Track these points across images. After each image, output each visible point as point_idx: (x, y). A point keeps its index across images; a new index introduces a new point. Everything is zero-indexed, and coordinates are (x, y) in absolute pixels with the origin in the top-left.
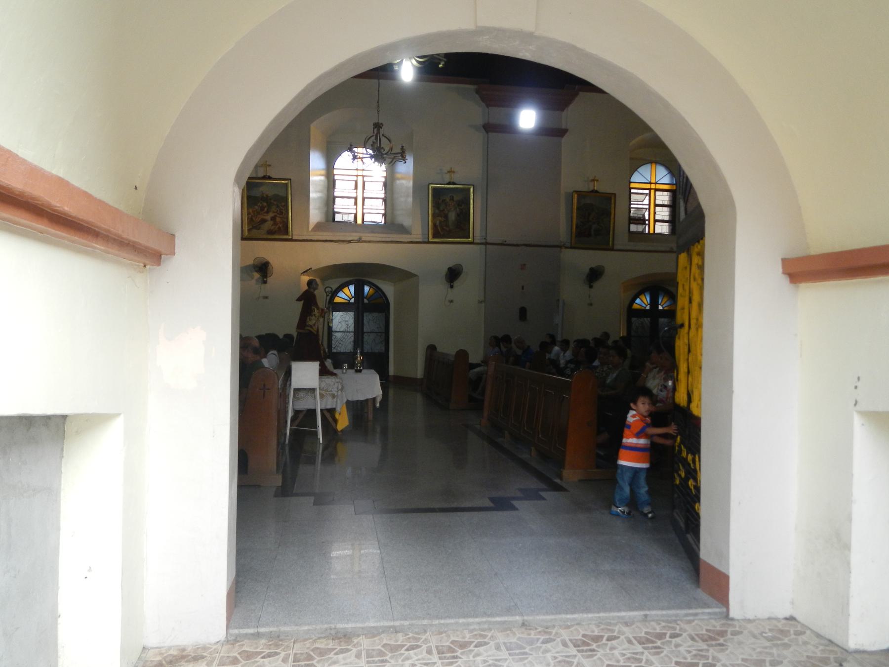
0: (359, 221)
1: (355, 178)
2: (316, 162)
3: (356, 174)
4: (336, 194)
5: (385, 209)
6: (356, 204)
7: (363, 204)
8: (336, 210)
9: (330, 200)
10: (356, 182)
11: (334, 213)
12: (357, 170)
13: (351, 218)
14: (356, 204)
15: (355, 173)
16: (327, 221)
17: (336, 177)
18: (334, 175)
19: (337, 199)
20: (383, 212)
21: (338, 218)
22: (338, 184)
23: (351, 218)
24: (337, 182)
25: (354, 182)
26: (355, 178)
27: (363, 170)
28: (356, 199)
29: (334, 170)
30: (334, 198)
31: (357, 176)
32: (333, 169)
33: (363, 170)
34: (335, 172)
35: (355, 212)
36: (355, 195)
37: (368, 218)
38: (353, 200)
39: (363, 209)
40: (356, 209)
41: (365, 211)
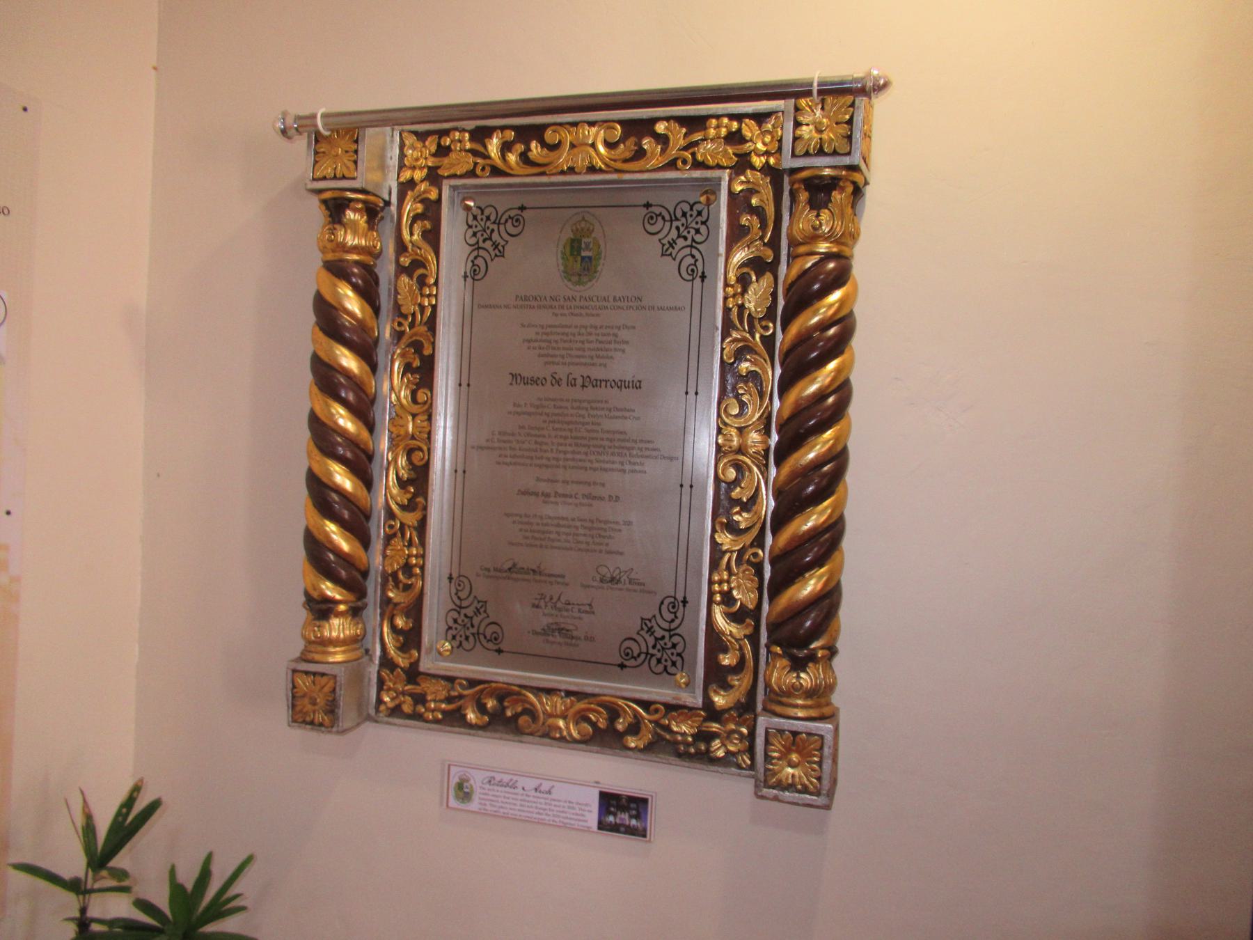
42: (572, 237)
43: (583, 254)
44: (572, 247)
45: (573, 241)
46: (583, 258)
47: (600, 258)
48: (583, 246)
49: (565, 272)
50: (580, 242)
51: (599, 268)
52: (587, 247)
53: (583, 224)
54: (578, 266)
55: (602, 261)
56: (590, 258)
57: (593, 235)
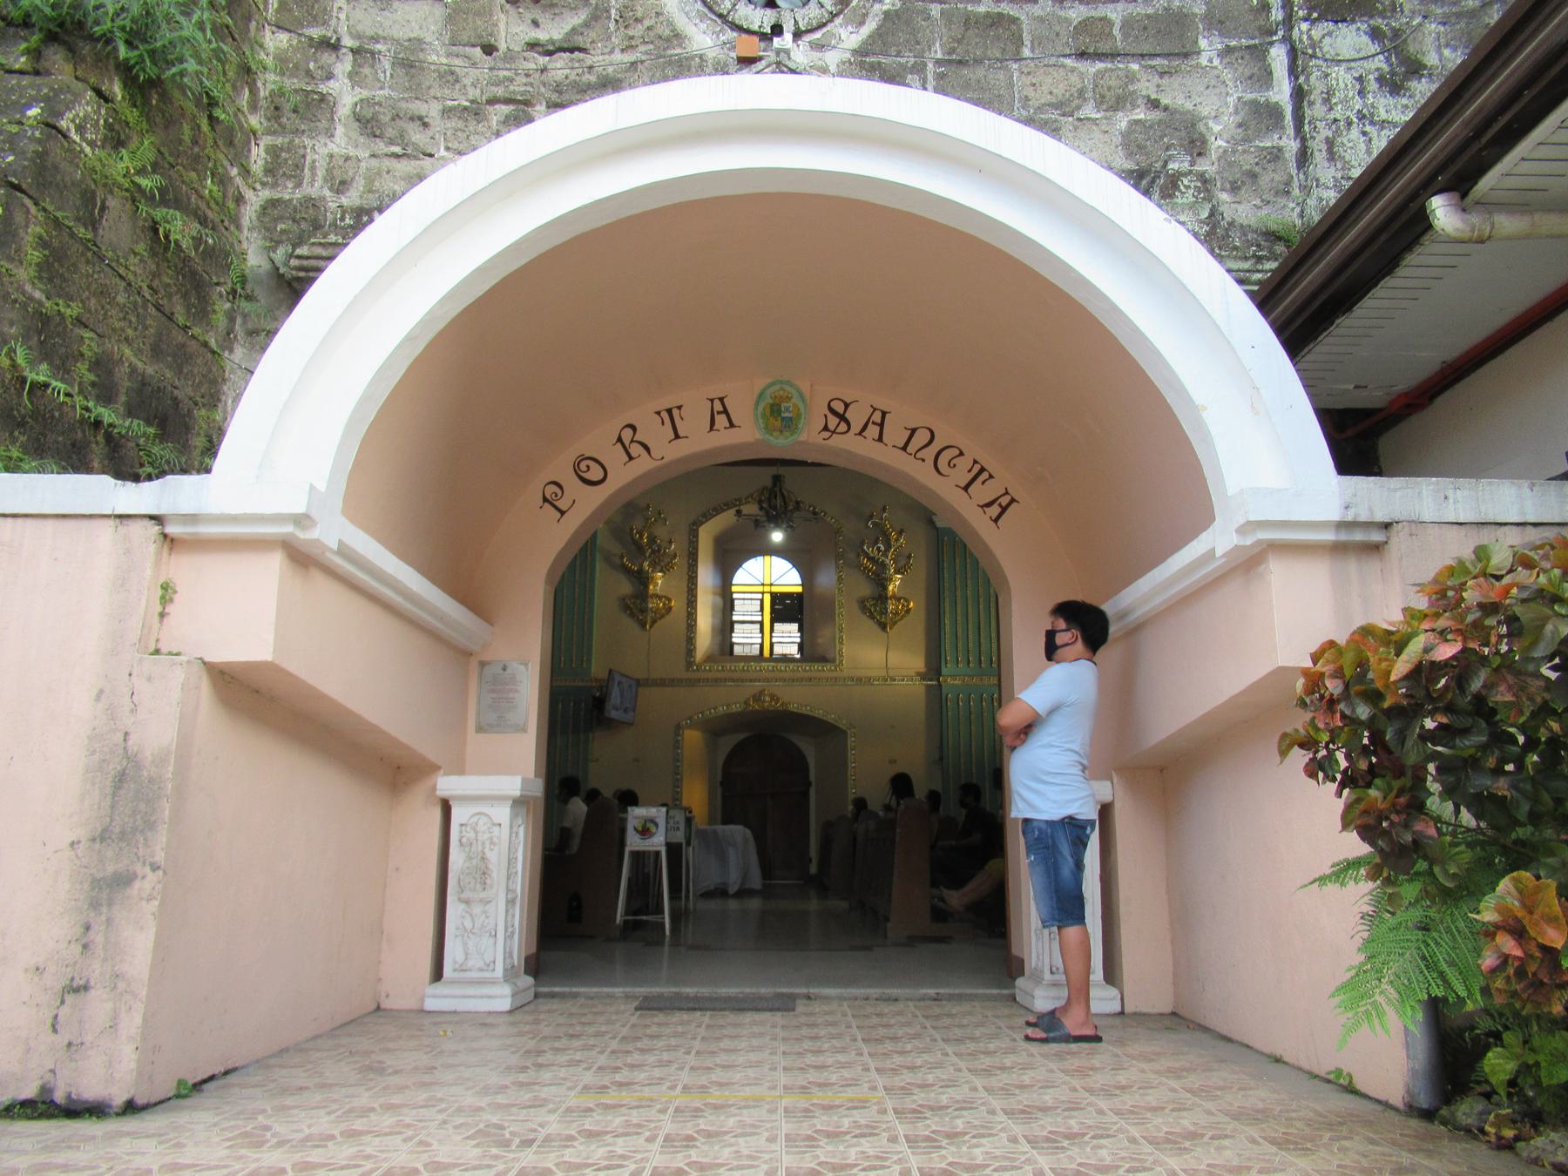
0: (766, 653)
1: (760, 596)
2: (706, 577)
4: (735, 618)
5: (801, 637)
6: (762, 631)
7: (772, 630)
9: (726, 626)
10: (762, 601)
11: (732, 645)
12: (763, 585)
13: (756, 652)
14: (762, 631)
15: (760, 589)
16: (722, 653)
17: (735, 596)
18: (732, 593)
19: (736, 626)
20: (798, 640)
21: (737, 650)
24: (736, 602)
25: (759, 602)
26: (760, 596)
27: (771, 585)
28: (761, 623)
30: (732, 623)
31: (763, 593)
32: (731, 585)
33: (771, 585)
34: (734, 589)
36: (759, 618)
37: (778, 650)
38: (758, 626)
39: (771, 637)
40: (762, 638)
41: (774, 640)
42: (771, 401)
43: (783, 415)
44: (772, 411)
45: (772, 405)
46: (783, 419)
47: (800, 418)
48: (783, 409)
49: (766, 428)
50: (779, 406)
51: (800, 426)
52: (787, 410)
53: (781, 393)
54: (778, 423)
55: (802, 420)
56: (791, 419)
57: (793, 401)
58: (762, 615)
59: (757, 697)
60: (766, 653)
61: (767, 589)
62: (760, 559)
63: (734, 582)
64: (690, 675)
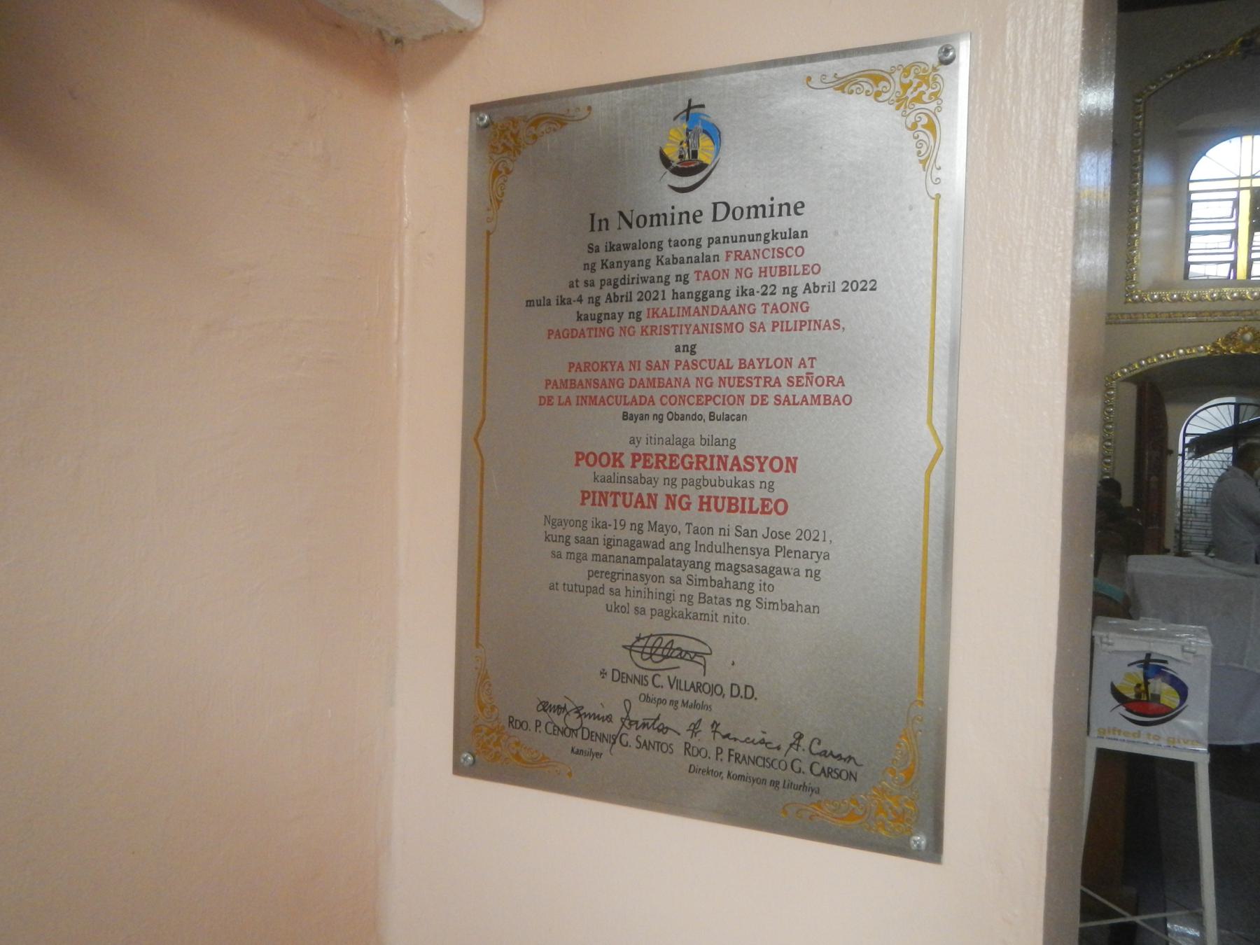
0: (1241, 274)
3: (1237, 186)
8: (1191, 259)
12: (1239, 178)
15: (1235, 184)
19: (1194, 239)
22: (1198, 211)
23: (1223, 271)
26: (1233, 195)
27: (1253, 177)
28: (1234, 234)
29: (1191, 185)
30: (1189, 235)
31: (1239, 190)
33: (1253, 177)
34: (1192, 187)
35: (1231, 258)
36: (1232, 226)
38: (1228, 237)
39: (1250, 252)
40: (1235, 253)
58: (1237, 221)
59: (1230, 338)
60: (1241, 274)
61: (1246, 183)
62: (1236, 141)
63: (1192, 178)
64: (1132, 308)
